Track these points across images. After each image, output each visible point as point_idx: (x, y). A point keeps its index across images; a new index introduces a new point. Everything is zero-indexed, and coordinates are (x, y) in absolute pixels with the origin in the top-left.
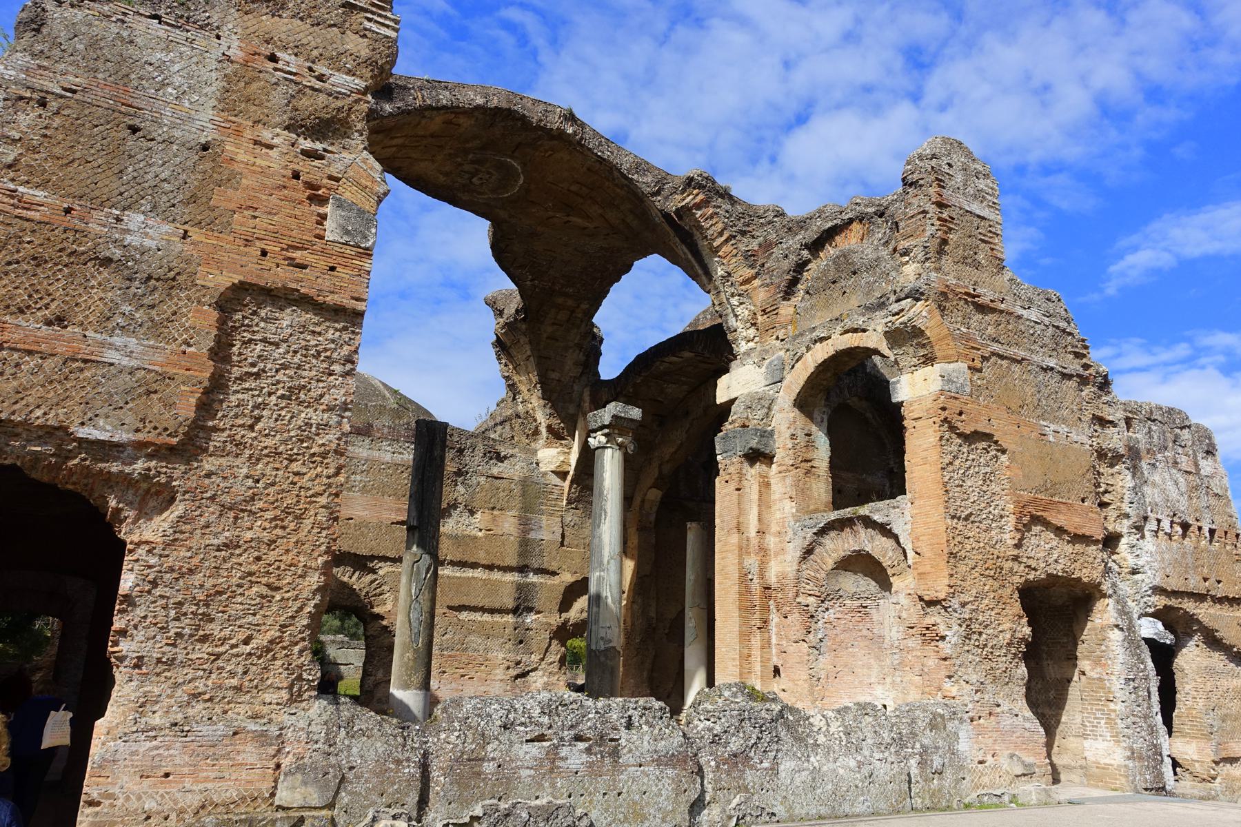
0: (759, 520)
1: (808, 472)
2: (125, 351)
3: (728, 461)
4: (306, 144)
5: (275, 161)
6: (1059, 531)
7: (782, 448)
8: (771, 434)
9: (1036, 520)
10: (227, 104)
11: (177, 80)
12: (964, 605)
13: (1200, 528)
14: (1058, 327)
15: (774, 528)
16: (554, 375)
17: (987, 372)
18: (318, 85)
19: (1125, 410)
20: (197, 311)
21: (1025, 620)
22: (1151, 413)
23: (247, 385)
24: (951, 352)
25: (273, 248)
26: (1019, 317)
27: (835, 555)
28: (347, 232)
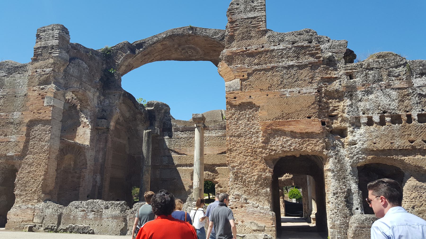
2: (13, 138)
4: (41, 87)
10: (29, 85)
18: (43, 73)
24: (231, 76)
25: (35, 111)
26: (273, 51)
28: (48, 103)
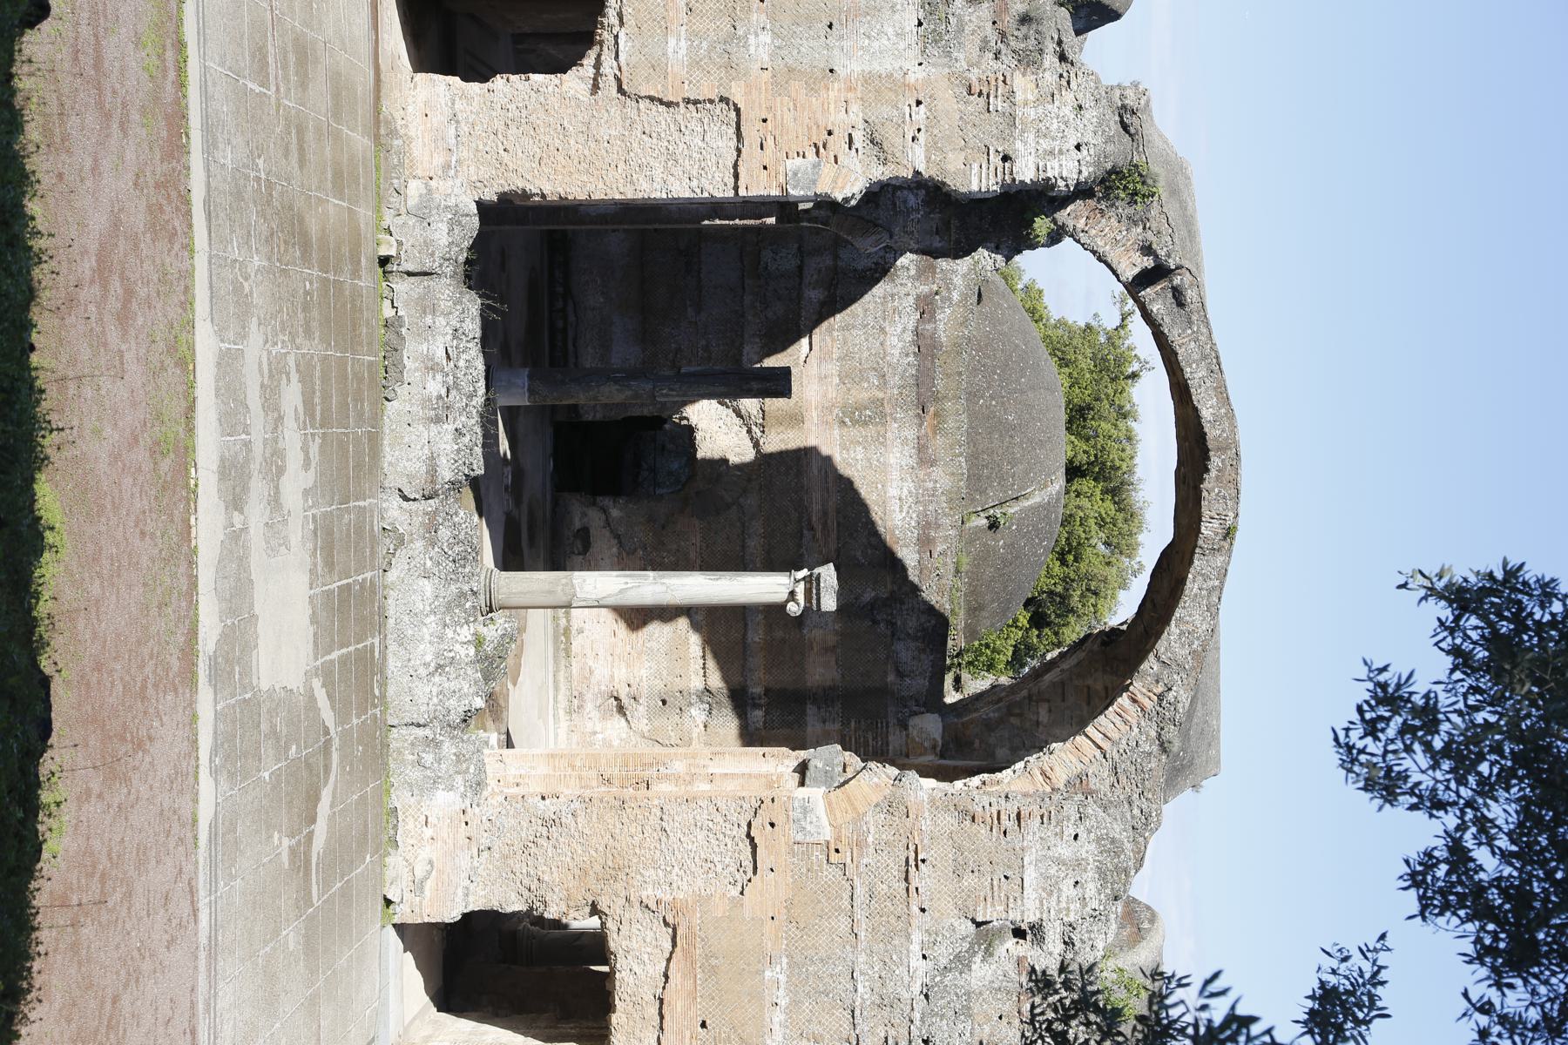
5: (837, 119)
10: (868, 79)
16: (1044, 715)
24: (838, 815)
26: (908, 937)
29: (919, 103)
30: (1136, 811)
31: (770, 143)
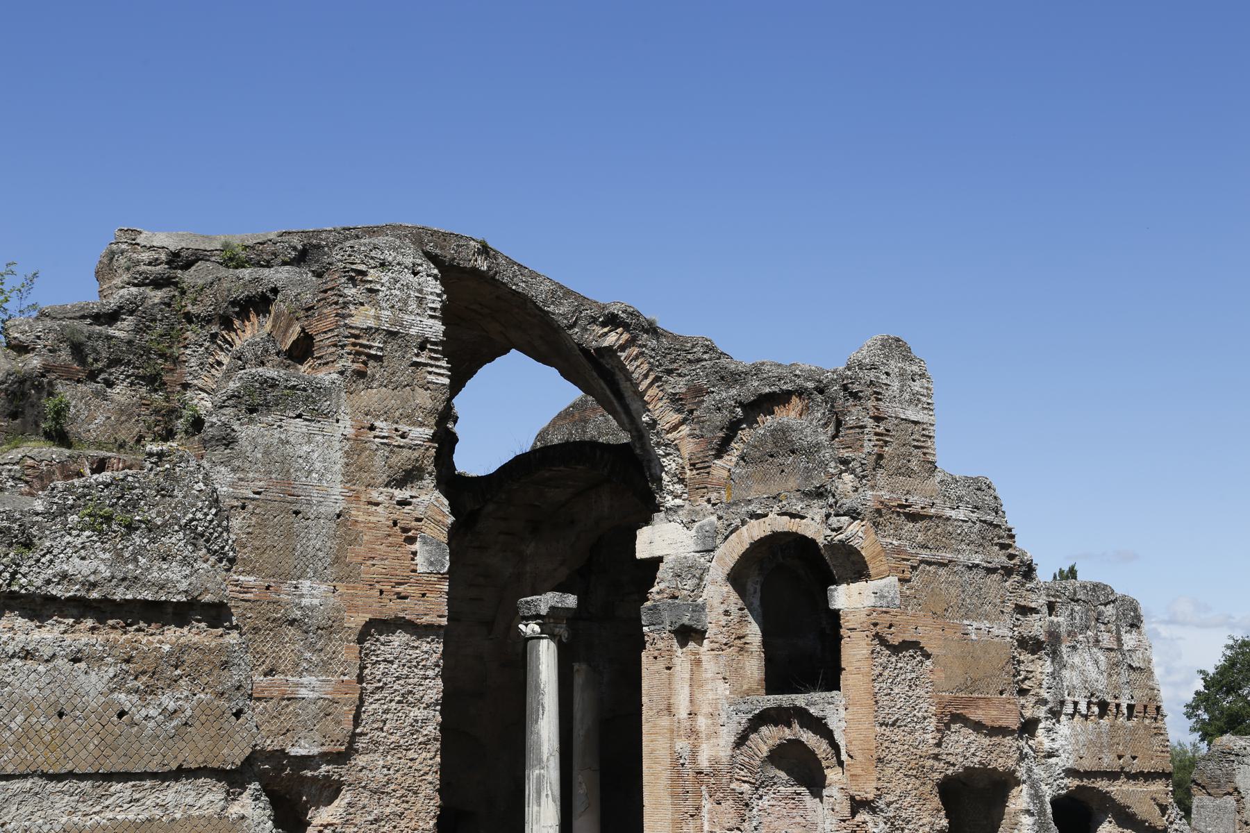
0: (691, 701)
1: (742, 649)
2: (311, 687)
3: (657, 640)
5: (381, 515)
6: (978, 727)
7: (713, 622)
8: (703, 607)
9: (956, 718)
10: (349, 479)
11: (318, 465)
12: (889, 804)
13: (1118, 706)
14: (985, 522)
15: (706, 709)
17: (915, 582)
18: (402, 442)
19: (1048, 595)
20: (348, 648)
21: (943, 813)
22: (1075, 593)
23: (376, 697)
24: (883, 568)
26: (948, 519)
27: (770, 742)
29: (372, 428)
30: (706, 356)
31: (400, 589)
